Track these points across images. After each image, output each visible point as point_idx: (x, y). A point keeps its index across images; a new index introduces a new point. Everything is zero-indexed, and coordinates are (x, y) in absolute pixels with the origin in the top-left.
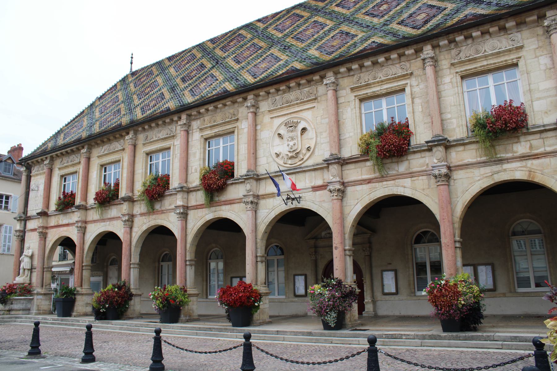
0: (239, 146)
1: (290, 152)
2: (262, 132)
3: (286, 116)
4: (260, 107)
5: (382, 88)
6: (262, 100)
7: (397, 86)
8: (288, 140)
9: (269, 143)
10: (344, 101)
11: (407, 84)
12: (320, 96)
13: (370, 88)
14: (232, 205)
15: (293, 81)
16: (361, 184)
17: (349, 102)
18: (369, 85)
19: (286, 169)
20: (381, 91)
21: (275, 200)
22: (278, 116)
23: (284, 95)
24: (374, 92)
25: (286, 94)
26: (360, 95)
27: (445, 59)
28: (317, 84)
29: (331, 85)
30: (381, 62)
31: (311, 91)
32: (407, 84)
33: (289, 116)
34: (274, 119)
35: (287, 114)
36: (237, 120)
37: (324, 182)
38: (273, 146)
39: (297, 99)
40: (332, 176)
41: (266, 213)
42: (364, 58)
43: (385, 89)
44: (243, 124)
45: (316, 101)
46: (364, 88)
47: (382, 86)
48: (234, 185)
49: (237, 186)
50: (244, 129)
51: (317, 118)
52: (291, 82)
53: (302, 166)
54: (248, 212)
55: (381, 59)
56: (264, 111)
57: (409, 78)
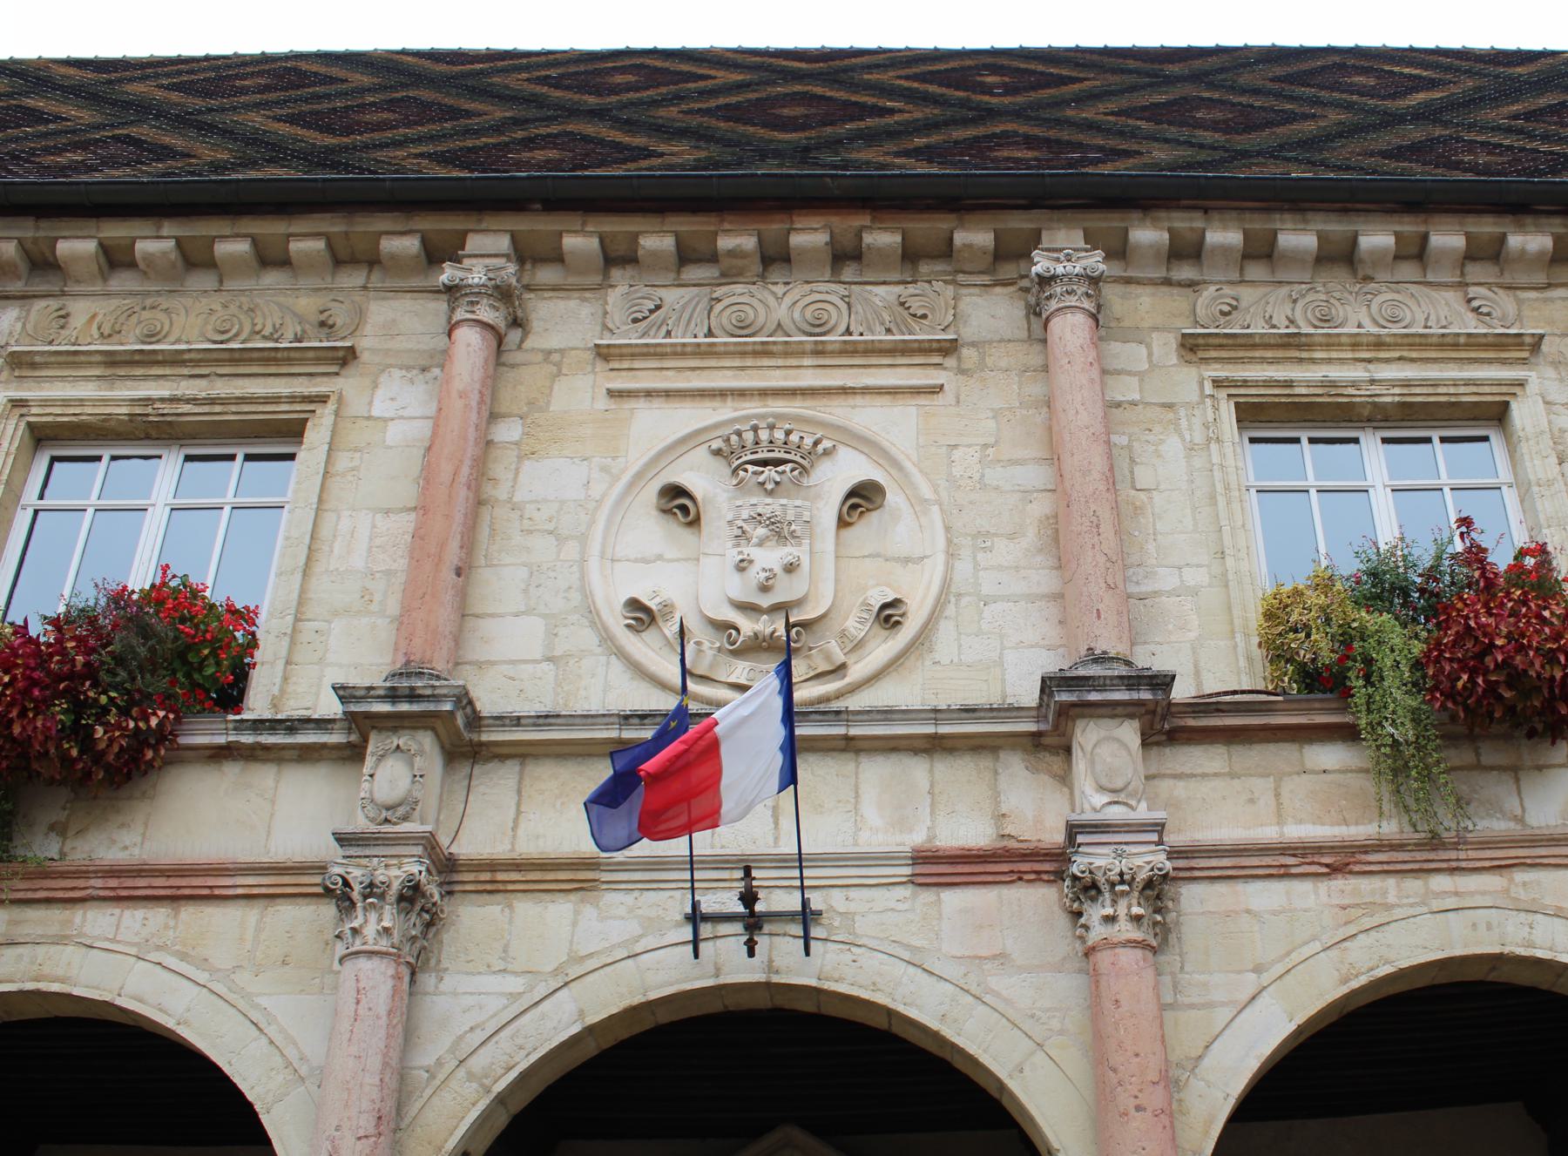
0: (329, 519)
3: (729, 402)
4: (536, 325)
5: (1378, 376)
6: (555, 289)
7: (1468, 382)
8: (742, 536)
9: (583, 539)
10: (1137, 397)
11: (1521, 384)
12: (973, 344)
13: (1301, 360)
17: (1169, 406)
18: (1299, 347)
20: (1376, 389)
21: (589, 911)
22: (668, 394)
23: (719, 292)
24: (1333, 384)
25: (739, 288)
26: (1245, 383)
28: (961, 277)
29: (1081, 290)
30: (1372, 252)
31: (916, 306)
32: (1521, 384)
33: (752, 408)
34: (640, 404)
35: (742, 394)
36: (347, 357)
38: (610, 559)
39: (818, 326)
40: (1102, 789)
42: (1281, 210)
43: (1393, 383)
44: (380, 393)
45: (950, 362)
46: (1269, 354)
47: (1370, 366)
48: (232, 771)
49: (264, 776)
50: (386, 420)
51: (957, 454)
52: (800, 222)
54: (364, 964)
55: (1377, 238)
56: (562, 351)
57: (1523, 361)
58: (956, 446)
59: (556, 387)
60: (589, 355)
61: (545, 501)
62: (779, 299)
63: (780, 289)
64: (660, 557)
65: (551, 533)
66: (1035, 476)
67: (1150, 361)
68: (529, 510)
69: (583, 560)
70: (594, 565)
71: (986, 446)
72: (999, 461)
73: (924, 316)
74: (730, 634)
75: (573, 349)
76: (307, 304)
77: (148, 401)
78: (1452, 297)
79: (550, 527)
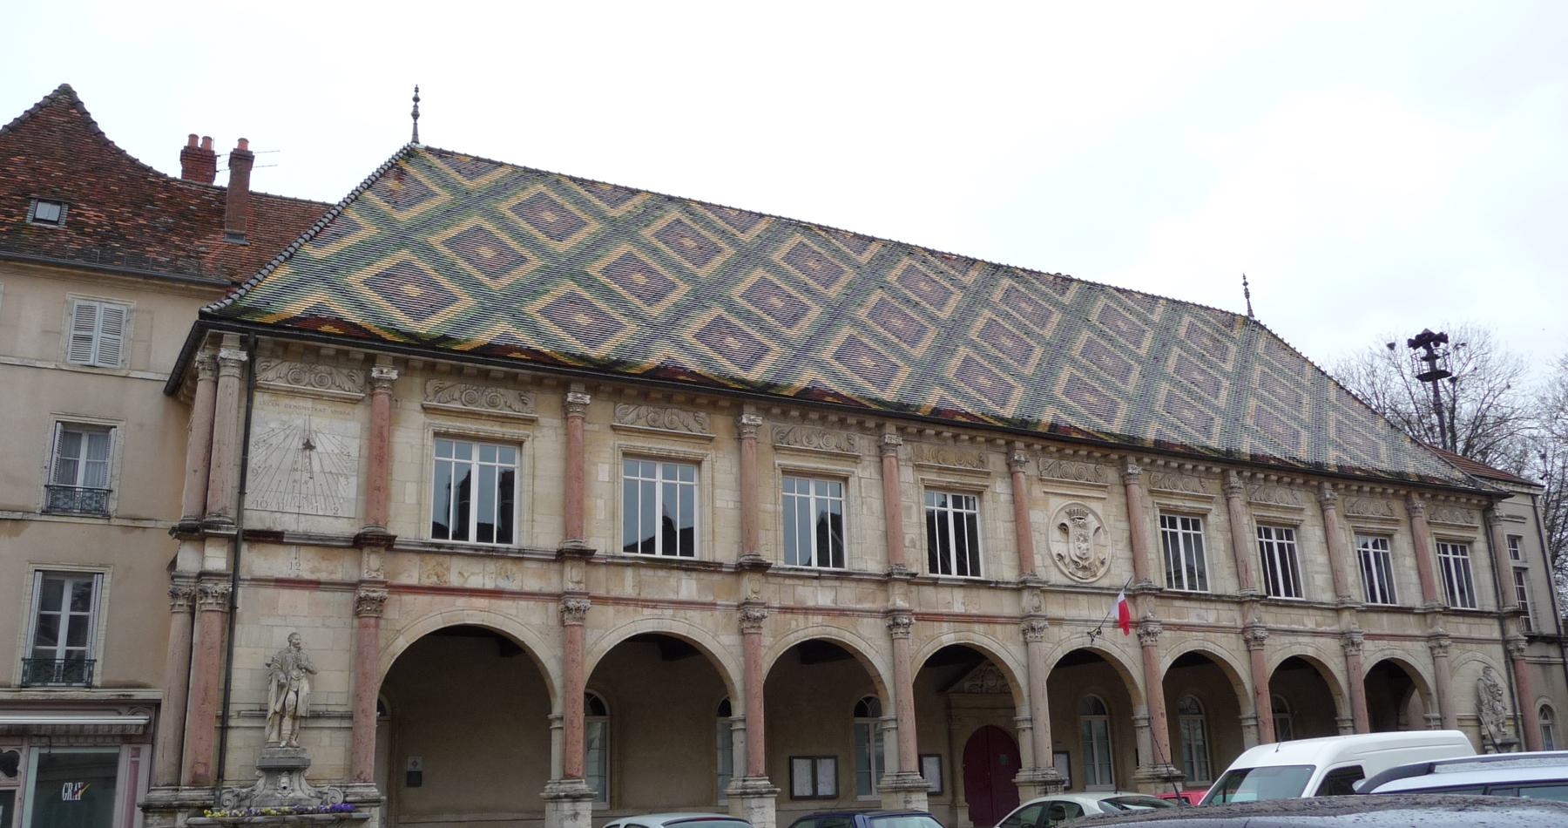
5: (1186, 505)
14: (992, 625)
15: (1085, 448)
16: (1171, 630)
17: (1146, 507)
19: (1074, 584)
22: (1056, 494)
24: (1177, 506)
34: (1050, 496)
41: (1048, 650)
52: (1083, 448)
53: (1096, 585)
60: (1036, 479)
66: (1124, 525)
69: (1047, 540)
70: (1050, 542)
76: (975, 452)
77: (950, 482)
78: (1197, 480)
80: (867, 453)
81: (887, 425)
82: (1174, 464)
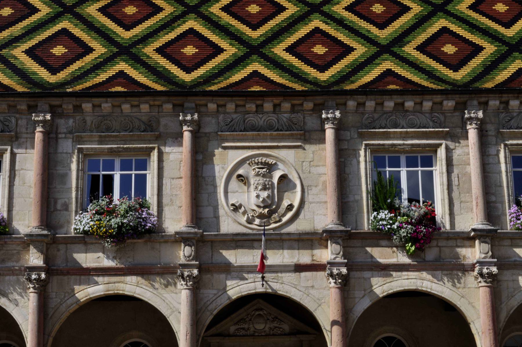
1: (259, 207)
2: (205, 166)
23: (247, 116)
27: (491, 123)
37: (313, 260)
51: (304, 163)
56: (209, 133)
58: (304, 162)
59: (209, 144)
61: (210, 176)
62: (261, 119)
63: (261, 116)
64: (237, 191)
65: (212, 185)
67: (350, 136)
68: (207, 178)
71: (311, 162)
72: (314, 166)
73: (296, 124)
74: (254, 213)
75: (212, 132)
79: (212, 183)
80: (24, 130)
81: (39, 104)
82: (427, 105)
